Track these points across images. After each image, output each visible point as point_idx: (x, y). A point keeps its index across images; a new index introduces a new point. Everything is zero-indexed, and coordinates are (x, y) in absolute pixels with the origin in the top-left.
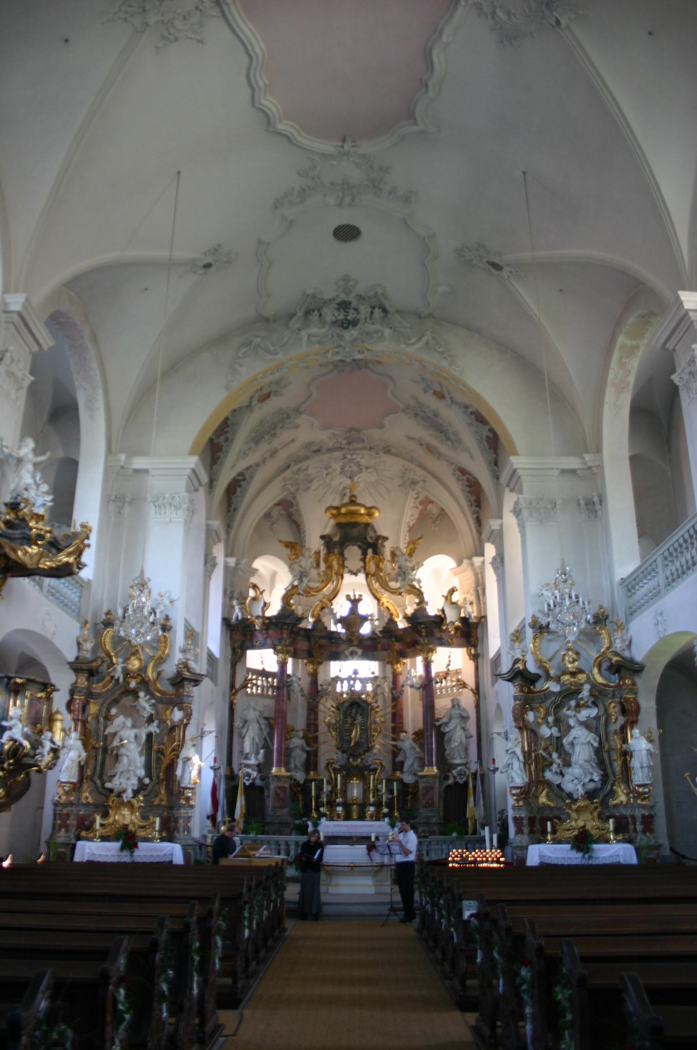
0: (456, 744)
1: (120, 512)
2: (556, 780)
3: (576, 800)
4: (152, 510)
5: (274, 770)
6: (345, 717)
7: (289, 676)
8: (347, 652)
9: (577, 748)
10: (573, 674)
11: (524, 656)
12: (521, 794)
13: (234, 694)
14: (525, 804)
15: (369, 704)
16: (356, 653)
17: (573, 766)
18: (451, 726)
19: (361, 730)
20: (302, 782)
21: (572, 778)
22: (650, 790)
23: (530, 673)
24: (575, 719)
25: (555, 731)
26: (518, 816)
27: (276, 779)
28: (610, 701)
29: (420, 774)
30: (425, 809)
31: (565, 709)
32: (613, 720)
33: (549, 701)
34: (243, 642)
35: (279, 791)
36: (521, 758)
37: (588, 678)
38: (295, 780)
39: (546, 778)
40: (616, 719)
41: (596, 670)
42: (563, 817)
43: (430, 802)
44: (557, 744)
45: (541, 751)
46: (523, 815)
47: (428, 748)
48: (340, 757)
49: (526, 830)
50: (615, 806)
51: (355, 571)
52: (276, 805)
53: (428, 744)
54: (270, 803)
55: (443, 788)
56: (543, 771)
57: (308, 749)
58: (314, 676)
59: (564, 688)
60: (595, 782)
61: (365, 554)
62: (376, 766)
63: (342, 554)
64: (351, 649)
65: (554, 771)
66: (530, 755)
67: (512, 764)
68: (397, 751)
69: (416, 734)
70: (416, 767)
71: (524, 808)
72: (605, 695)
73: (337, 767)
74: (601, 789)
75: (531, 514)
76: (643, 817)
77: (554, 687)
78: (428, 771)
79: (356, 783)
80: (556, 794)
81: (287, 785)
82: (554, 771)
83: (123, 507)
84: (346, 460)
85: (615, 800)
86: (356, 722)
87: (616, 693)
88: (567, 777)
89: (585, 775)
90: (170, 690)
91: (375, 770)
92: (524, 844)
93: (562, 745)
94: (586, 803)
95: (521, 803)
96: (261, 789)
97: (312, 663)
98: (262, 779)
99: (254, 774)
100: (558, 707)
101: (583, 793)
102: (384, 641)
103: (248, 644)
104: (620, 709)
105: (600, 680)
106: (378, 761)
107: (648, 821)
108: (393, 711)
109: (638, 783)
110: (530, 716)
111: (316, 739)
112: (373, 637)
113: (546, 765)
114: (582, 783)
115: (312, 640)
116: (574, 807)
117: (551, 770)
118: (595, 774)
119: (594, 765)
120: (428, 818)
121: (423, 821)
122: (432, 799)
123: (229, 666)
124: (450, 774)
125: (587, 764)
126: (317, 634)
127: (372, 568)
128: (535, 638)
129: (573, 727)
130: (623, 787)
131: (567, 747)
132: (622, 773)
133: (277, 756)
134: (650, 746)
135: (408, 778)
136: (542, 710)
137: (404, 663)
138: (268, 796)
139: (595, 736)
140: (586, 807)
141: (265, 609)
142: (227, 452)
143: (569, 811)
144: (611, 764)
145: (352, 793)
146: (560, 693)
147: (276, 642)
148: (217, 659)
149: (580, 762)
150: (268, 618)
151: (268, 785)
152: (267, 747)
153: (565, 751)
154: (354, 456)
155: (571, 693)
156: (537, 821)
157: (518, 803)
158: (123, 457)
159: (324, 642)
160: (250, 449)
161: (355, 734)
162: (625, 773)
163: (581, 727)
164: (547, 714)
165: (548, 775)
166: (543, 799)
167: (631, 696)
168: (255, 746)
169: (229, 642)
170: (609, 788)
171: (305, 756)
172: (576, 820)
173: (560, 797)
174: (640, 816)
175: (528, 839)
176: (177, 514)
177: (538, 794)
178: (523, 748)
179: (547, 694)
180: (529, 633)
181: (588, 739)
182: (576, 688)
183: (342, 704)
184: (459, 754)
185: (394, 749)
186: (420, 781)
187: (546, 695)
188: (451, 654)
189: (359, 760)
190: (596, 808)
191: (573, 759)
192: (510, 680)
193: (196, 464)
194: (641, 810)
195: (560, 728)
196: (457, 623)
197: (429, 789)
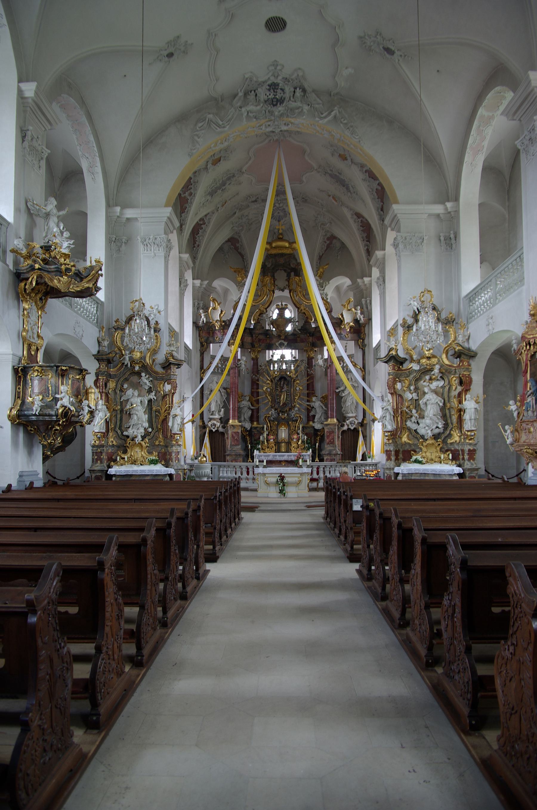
0: (350, 404)
1: (119, 250)
2: (414, 426)
3: (427, 440)
4: (141, 247)
5: (231, 421)
6: (276, 387)
7: (239, 360)
8: (277, 344)
10: (429, 358)
11: (396, 346)
12: (391, 436)
15: (292, 378)
16: (283, 344)
17: (425, 418)
18: (346, 393)
19: (287, 395)
20: (249, 429)
21: (424, 426)
22: (475, 434)
23: (400, 357)
24: (429, 388)
25: (415, 396)
26: (388, 449)
28: (452, 376)
29: (325, 423)
30: (328, 445)
31: (422, 381)
32: (454, 389)
33: (412, 376)
34: (208, 338)
36: (392, 413)
37: (439, 361)
38: (244, 428)
39: (408, 426)
40: (456, 388)
41: (444, 356)
42: (418, 450)
44: (416, 403)
45: (405, 409)
46: (392, 449)
47: (331, 407)
48: (274, 413)
49: (393, 458)
50: (452, 443)
51: (282, 288)
52: (233, 443)
53: (331, 405)
55: (340, 432)
56: (406, 421)
57: (253, 408)
58: (255, 361)
59: (422, 367)
60: (439, 428)
61: (289, 276)
62: (297, 418)
63: (273, 276)
64: (280, 341)
65: (413, 421)
66: (397, 411)
68: (310, 408)
69: (322, 397)
70: (323, 418)
71: (392, 444)
72: (450, 373)
73: (272, 419)
74: (443, 433)
75: (405, 247)
76: (469, 450)
77: (415, 367)
78: (331, 421)
80: (414, 436)
81: (240, 431)
82: (413, 421)
83: (121, 246)
84: (275, 207)
86: (283, 390)
87: (457, 371)
88: (421, 425)
90: (159, 369)
91: (297, 421)
92: (392, 467)
93: (419, 405)
94: (433, 441)
95: (391, 441)
96: (223, 434)
97: (254, 351)
98: (224, 427)
100: (417, 380)
101: (431, 436)
102: (302, 336)
103: (211, 339)
104: (459, 381)
105: (446, 362)
106: (298, 415)
107: (472, 454)
108: (308, 383)
109: (468, 429)
110: (399, 386)
111: (258, 401)
112: (294, 333)
113: (408, 418)
114: (431, 429)
115: (254, 336)
116: (424, 444)
118: (440, 423)
119: (440, 418)
120: (330, 451)
121: (327, 453)
122: (333, 439)
124: (345, 423)
125: (434, 417)
126: (257, 332)
127: (294, 286)
128: (404, 334)
129: (427, 393)
130: (457, 432)
131: (422, 406)
132: (457, 423)
133: (232, 413)
134: (477, 406)
135: (318, 426)
136: (406, 381)
137: (315, 351)
138: (228, 438)
140: (433, 444)
141: (222, 315)
142: (191, 203)
143: (422, 447)
144: (450, 417)
145: (282, 436)
146: (419, 370)
149: (430, 416)
150: (224, 321)
151: (227, 431)
152: (225, 406)
153: (421, 409)
154: (281, 205)
155: (426, 371)
156: (401, 452)
158: (118, 209)
159: (261, 337)
160: (207, 201)
161: (283, 397)
163: (432, 393)
164: (410, 385)
165: (409, 424)
166: (405, 439)
167: (467, 373)
168: (218, 406)
169: (198, 338)
170: (448, 432)
171: (250, 412)
172: (425, 452)
173: (416, 438)
174: (467, 450)
175: (394, 464)
176: (159, 250)
177: (402, 436)
178: (393, 406)
179: (410, 371)
180: (400, 330)
181: (437, 401)
182: (430, 368)
183: (274, 378)
184: (351, 411)
185: (309, 407)
186: (325, 428)
188: (347, 345)
189: (286, 414)
190: (439, 445)
191: (426, 414)
192: (386, 362)
193: (170, 213)
194: (468, 446)
195: (418, 394)
196: (352, 324)
197: (332, 432)
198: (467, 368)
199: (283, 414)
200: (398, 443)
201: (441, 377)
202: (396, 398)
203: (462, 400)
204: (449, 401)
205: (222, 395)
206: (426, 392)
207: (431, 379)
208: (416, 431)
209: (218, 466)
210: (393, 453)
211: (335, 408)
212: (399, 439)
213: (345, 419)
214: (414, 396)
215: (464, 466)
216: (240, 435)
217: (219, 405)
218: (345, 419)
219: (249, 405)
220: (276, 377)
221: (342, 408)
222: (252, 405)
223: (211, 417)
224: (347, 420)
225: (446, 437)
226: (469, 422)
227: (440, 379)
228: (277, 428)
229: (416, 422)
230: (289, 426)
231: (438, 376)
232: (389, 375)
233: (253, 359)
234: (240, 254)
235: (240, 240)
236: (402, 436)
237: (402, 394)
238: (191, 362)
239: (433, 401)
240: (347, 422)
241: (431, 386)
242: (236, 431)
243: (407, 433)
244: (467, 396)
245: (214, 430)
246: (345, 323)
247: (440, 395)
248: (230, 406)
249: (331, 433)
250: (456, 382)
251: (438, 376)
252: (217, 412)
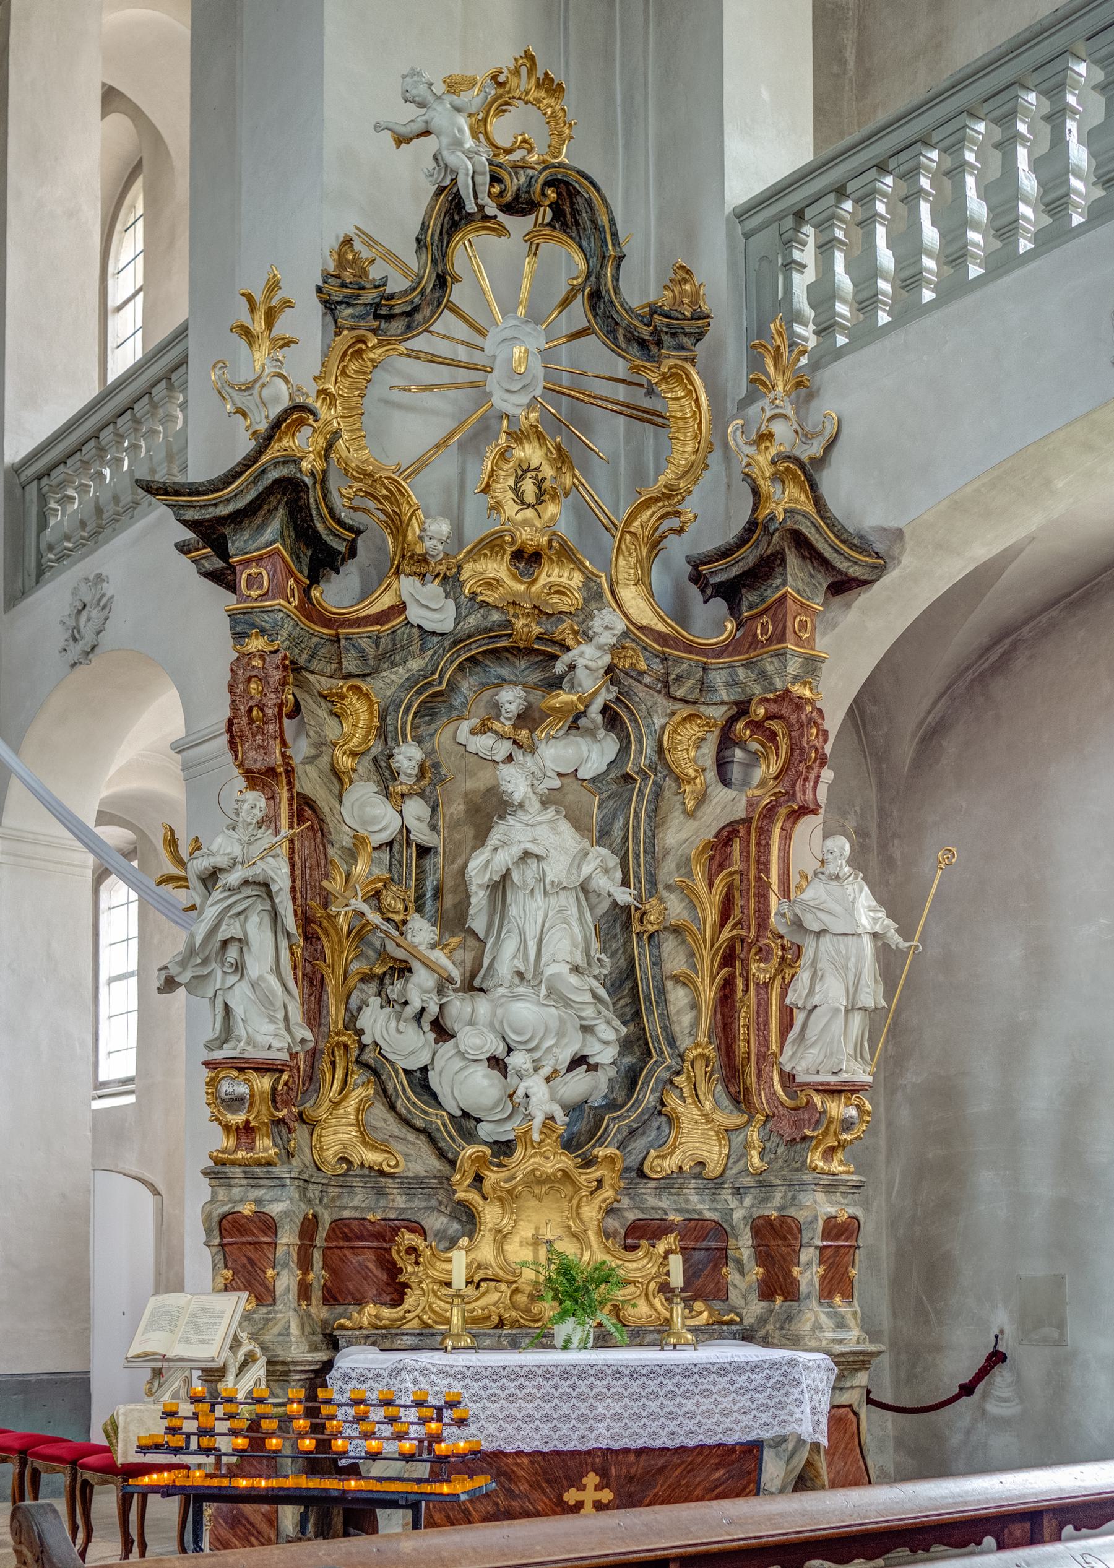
26: (247, 1209)
33: (394, 677)
46: (275, 1209)
50: (671, 1182)
59: (472, 621)
60: (594, 1067)
67: (242, 942)
94: (560, 1161)
125: (574, 980)
136: (357, 706)
143: (473, 1197)
146: (457, 641)
157: (251, 1148)
170: (649, 1099)
181: (586, 870)
206: (517, 797)
214: (411, 823)
232: (239, 636)
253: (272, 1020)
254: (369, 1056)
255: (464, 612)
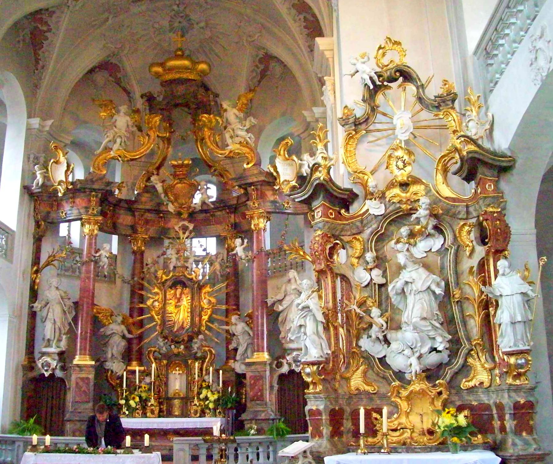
3: (409, 383)
9: (411, 299)
10: (404, 185)
13: (37, 272)
14: (326, 390)
17: (403, 329)
21: (401, 348)
22: (527, 361)
25: (377, 276)
27: (77, 369)
28: (462, 223)
31: (393, 242)
32: (468, 254)
33: (368, 231)
35: (81, 383)
36: (321, 318)
39: (363, 349)
41: (440, 177)
43: (259, 394)
45: (354, 307)
46: (321, 407)
48: (162, 344)
50: (471, 390)
52: (78, 399)
54: (70, 397)
56: (358, 338)
59: (391, 208)
64: (181, 224)
65: (374, 336)
67: (305, 326)
72: (454, 216)
76: (517, 406)
79: (179, 374)
80: (378, 375)
81: (91, 376)
82: (374, 336)
85: (471, 380)
87: (471, 209)
88: (394, 345)
89: (423, 343)
93: (388, 297)
94: (424, 385)
96: (62, 380)
98: (63, 368)
99: (54, 364)
101: (418, 370)
104: (478, 235)
105: (446, 192)
106: (207, 349)
109: (509, 350)
110: (341, 256)
113: (364, 329)
114: (417, 354)
116: (404, 393)
117: (369, 337)
118: (439, 339)
119: (438, 325)
121: (251, 416)
122: (261, 390)
123: (32, 241)
124: (284, 361)
125: (423, 323)
128: (349, 137)
129: (405, 267)
130: (483, 359)
131: (395, 299)
132: (482, 337)
134: (526, 288)
135: (239, 368)
139: (438, 279)
140: (423, 393)
144: (465, 324)
145: (175, 386)
147: (82, 211)
148: (13, 231)
149: (414, 320)
152: (72, 333)
153: (392, 306)
162: (486, 337)
163: (417, 266)
164: (365, 250)
165: (365, 344)
167: (495, 210)
168: (57, 330)
171: (123, 343)
172: (407, 414)
173: (384, 378)
181: (428, 284)
182: (409, 207)
187: (365, 222)
189: (182, 347)
190: (440, 393)
191: (404, 318)
194: (513, 394)
195: (385, 272)
196: (294, 183)
197: (259, 378)
198: (493, 197)
199: (177, 345)
200: (340, 391)
201: (436, 228)
202: (334, 282)
203: (490, 277)
204: (457, 284)
205: (64, 312)
206: (402, 264)
207: (412, 235)
208: (382, 360)
209: (24, 442)
210: (324, 418)
211: (265, 332)
212: (343, 382)
213: (285, 352)
215: (506, 449)
216: (92, 384)
217: (60, 329)
218: (285, 352)
219: (122, 331)
220: (166, 280)
221: (280, 333)
222: (130, 332)
223: (44, 350)
224: (288, 355)
225: (456, 373)
226: (509, 330)
227: (432, 231)
228: (167, 370)
229: (381, 338)
230: (187, 365)
231: (427, 224)
233: (134, 252)
234: (125, 90)
235: (120, 65)
236: (348, 375)
237: (349, 274)
238: (12, 255)
239: (419, 285)
240: (288, 358)
241: (413, 250)
242: (84, 376)
243: (362, 368)
244: (499, 263)
245: (47, 374)
246: (282, 180)
247: (437, 271)
248: (77, 330)
249: (258, 380)
250: (472, 235)
251: (427, 224)
252: (55, 341)
253: (316, 348)
254: (365, 355)
255: (388, 206)
